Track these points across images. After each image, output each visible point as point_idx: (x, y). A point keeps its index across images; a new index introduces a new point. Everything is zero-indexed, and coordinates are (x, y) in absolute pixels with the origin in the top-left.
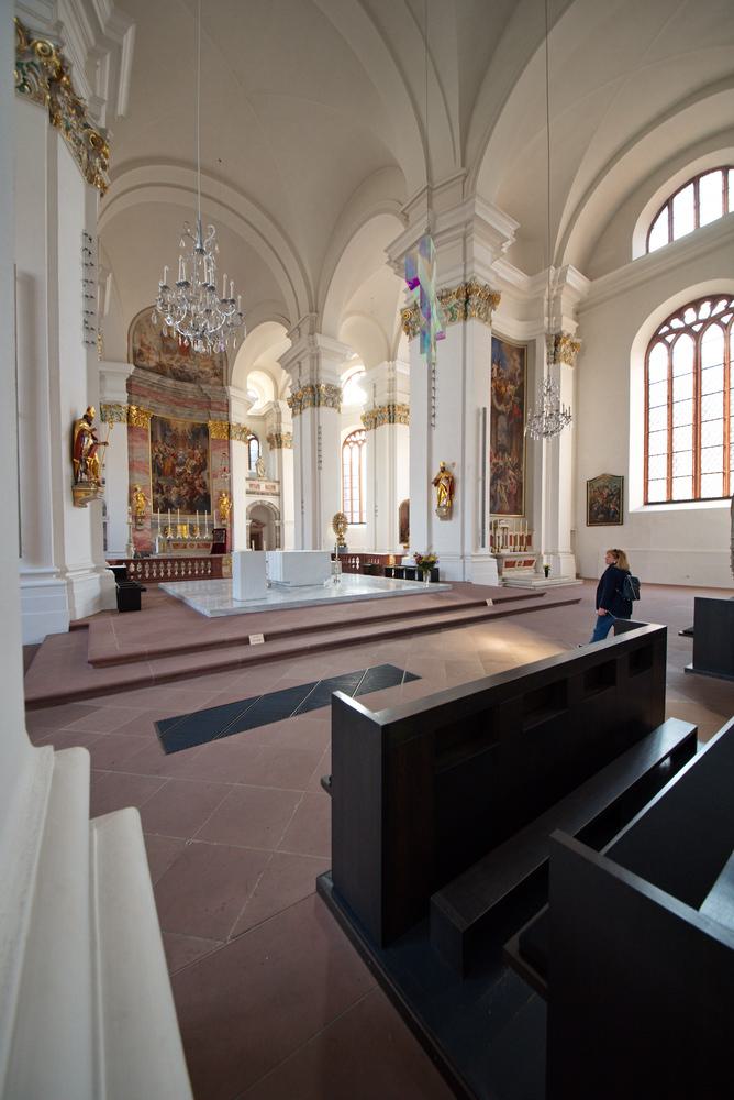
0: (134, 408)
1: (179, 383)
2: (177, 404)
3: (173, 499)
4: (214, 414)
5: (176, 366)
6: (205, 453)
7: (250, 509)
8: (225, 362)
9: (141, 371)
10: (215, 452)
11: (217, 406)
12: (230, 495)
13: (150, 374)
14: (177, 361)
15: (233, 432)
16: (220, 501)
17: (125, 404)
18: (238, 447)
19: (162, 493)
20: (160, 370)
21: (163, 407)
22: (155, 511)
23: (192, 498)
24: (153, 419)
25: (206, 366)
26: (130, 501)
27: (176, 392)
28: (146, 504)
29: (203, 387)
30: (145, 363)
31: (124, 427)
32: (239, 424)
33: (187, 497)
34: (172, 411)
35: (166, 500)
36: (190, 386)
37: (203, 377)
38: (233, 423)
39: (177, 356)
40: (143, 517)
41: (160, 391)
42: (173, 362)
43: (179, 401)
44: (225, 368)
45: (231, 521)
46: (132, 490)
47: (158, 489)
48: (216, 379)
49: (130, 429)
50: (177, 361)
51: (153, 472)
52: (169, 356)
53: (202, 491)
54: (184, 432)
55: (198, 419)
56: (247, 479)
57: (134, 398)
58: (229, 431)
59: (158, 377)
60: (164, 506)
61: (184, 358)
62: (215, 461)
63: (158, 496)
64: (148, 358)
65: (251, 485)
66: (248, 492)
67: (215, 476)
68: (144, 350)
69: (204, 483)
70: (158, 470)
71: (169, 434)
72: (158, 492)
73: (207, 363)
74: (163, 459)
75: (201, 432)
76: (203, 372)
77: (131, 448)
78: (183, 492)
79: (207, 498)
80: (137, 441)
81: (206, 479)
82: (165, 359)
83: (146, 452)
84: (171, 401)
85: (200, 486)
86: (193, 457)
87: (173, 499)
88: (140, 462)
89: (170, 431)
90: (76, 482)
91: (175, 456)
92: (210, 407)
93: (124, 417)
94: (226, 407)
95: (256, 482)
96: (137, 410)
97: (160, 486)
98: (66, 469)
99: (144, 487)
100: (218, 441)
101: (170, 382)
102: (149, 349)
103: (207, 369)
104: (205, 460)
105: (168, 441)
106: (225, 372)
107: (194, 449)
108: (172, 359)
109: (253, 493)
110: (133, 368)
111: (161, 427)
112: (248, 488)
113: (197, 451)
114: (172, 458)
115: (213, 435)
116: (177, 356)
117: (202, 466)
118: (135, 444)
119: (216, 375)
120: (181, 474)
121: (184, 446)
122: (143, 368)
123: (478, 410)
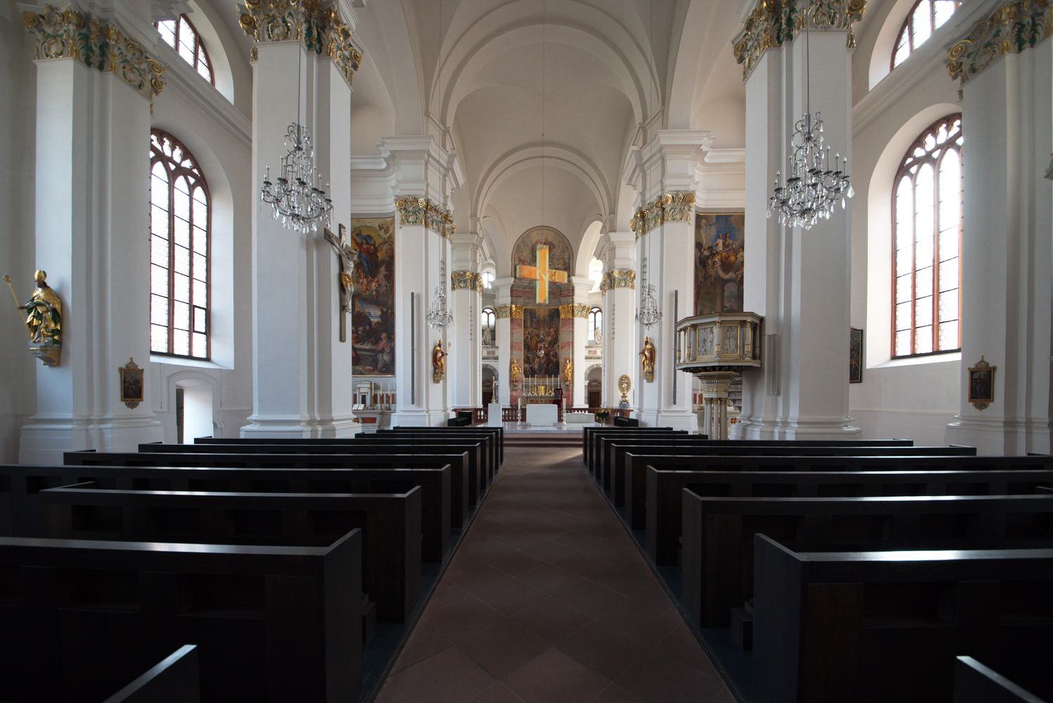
0: (513, 306)
3: (536, 367)
6: (557, 332)
10: (564, 329)
15: (576, 313)
16: (565, 366)
17: (509, 305)
18: (578, 321)
26: (511, 370)
31: (509, 319)
32: (580, 304)
33: (545, 365)
35: (532, 368)
38: (576, 305)
40: (517, 381)
45: (573, 382)
46: (512, 363)
47: (527, 360)
49: (511, 320)
51: (525, 348)
53: (554, 360)
56: (586, 347)
58: (573, 311)
60: (530, 373)
62: (563, 337)
63: (526, 366)
65: (589, 352)
67: (563, 348)
70: (528, 347)
78: (543, 361)
79: (557, 364)
83: (520, 337)
85: (553, 356)
86: (548, 335)
87: (536, 367)
89: (536, 317)
91: (538, 336)
95: (593, 349)
99: (518, 360)
105: (534, 325)
112: (587, 355)
115: (562, 316)
117: (555, 341)
121: (544, 327)
123: (671, 294)
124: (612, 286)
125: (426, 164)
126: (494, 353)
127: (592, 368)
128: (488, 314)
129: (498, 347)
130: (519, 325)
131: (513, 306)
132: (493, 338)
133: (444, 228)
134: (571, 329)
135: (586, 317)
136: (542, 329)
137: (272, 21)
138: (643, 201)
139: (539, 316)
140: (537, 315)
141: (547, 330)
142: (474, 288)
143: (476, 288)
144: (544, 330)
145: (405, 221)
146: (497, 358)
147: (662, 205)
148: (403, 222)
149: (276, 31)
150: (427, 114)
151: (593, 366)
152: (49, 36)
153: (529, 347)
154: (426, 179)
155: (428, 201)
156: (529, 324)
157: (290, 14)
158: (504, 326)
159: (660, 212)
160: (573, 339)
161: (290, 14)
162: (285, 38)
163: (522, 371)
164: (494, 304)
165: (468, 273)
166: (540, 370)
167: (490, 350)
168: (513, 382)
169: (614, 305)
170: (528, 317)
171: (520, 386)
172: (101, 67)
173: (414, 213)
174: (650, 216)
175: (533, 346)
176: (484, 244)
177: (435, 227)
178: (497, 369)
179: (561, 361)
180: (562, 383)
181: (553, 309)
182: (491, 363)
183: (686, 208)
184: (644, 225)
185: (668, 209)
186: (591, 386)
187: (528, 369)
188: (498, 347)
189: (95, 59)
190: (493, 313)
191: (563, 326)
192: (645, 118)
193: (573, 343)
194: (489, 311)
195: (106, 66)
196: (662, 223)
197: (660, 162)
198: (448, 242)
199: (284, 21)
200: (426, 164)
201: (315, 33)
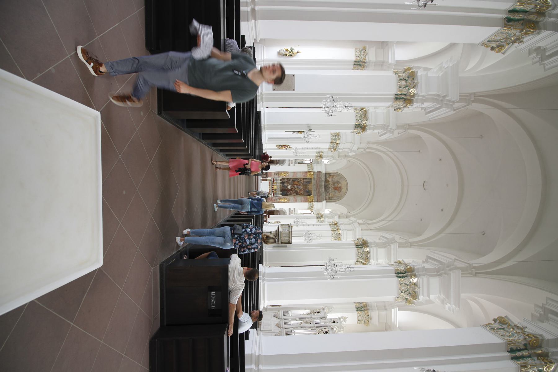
0: (313, 173)
1: (324, 186)
2: (317, 186)
3: (285, 185)
4: (316, 197)
5: (330, 186)
6: (302, 194)
7: (283, 210)
8: (334, 201)
9: (324, 175)
10: (303, 198)
11: (319, 198)
12: (288, 202)
13: (324, 178)
14: (331, 186)
17: (313, 171)
18: (306, 204)
19: (287, 181)
20: (326, 181)
21: (315, 182)
22: (281, 180)
23: (286, 190)
24: (311, 179)
25: (332, 195)
26: (284, 172)
27: (321, 186)
28: (283, 176)
29: (324, 193)
30: (327, 177)
31: (307, 171)
32: (314, 205)
33: (286, 189)
34: (314, 185)
35: (285, 182)
36: (323, 189)
37: (328, 194)
38: (313, 203)
39: (333, 186)
40: (279, 175)
41: (320, 181)
42: (330, 185)
43: (318, 187)
44: (332, 201)
47: (288, 180)
48: (328, 198)
49: (306, 172)
50: (331, 186)
51: (294, 179)
52: (332, 184)
53: (289, 193)
54: (308, 188)
55: (313, 192)
56: (295, 209)
57: (316, 173)
58: (310, 202)
59: (324, 180)
60: (283, 182)
61: (333, 188)
62: (299, 197)
63: (286, 180)
64: (329, 178)
65: (293, 210)
66: (290, 209)
67: (294, 197)
68: (332, 176)
69: (292, 194)
70: (295, 180)
71: (307, 183)
72: (287, 180)
73: (333, 195)
74: (298, 182)
75: (309, 193)
76: (329, 194)
77: (300, 172)
79: (287, 195)
80: (303, 174)
81: (293, 195)
82: (330, 182)
83: (299, 176)
84: (318, 184)
85: (290, 193)
86: (300, 190)
87: (285, 185)
88: (296, 175)
90: (280, 146)
91: (300, 185)
92: (318, 196)
93: (309, 171)
94: (319, 201)
96: (312, 174)
97: (289, 181)
98: (281, 144)
99: (288, 175)
100: (307, 199)
101: (324, 184)
102: (332, 178)
103: (331, 195)
104: (300, 194)
105: (305, 183)
106: (331, 201)
107: (303, 191)
108: (331, 185)
109: (290, 211)
110: (325, 173)
111: (309, 181)
112: (291, 209)
113: (302, 192)
114: (299, 184)
115: (308, 197)
116: (333, 186)
117: (297, 193)
118: (302, 173)
119: (330, 198)
120: (294, 187)
122: (325, 176)
124: (318, 217)
125: (352, 143)
126: (292, 164)
127: (285, 212)
128: (310, 160)
129: (294, 165)
130: (304, 176)
131: (313, 173)
132: (299, 163)
133: (332, 148)
134: (303, 201)
135: (308, 209)
136: (303, 187)
137: (361, 116)
138: (341, 224)
139: (309, 186)
140: (309, 185)
141: (302, 190)
142: (317, 156)
143: (317, 157)
144: (303, 188)
145: (333, 135)
146: (289, 165)
147: (337, 230)
148: (332, 134)
149: (358, 117)
150: (369, 143)
151: (286, 212)
152: (361, 52)
153: (294, 181)
154: (347, 143)
155: (339, 144)
156: (304, 181)
157: (362, 121)
158: (303, 168)
159: (335, 229)
160: (298, 202)
161: (362, 121)
162: (357, 120)
163: (284, 177)
164: (314, 163)
165: (322, 154)
166: (284, 187)
167: (293, 162)
168: (278, 173)
169: (310, 219)
170: (308, 181)
171: (276, 177)
172: (355, 64)
173: (335, 139)
174: (335, 226)
175: (295, 183)
176: (334, 161)
177: (331, 146)
178: (285, 165)
179: (288, 197)
180: (278, 198)
181: (312, 192)
182: (287, 163)
183: (336, 239)
184: (333, 225)
185: (336, 232)
186: (277, 212)
187: (284, 181)
188: (294, 165)
189: (355, 63)
190: (311, 163)
191: (304, 197)
192: (368, 224)
193: (296, 202)
194: (312, 160)
195: (355, 65)
196: (332, 230)
197: (352, 229)
198: (327, 150)
199: (361, 119)
200: (352, 143)
201: (359, 126)
